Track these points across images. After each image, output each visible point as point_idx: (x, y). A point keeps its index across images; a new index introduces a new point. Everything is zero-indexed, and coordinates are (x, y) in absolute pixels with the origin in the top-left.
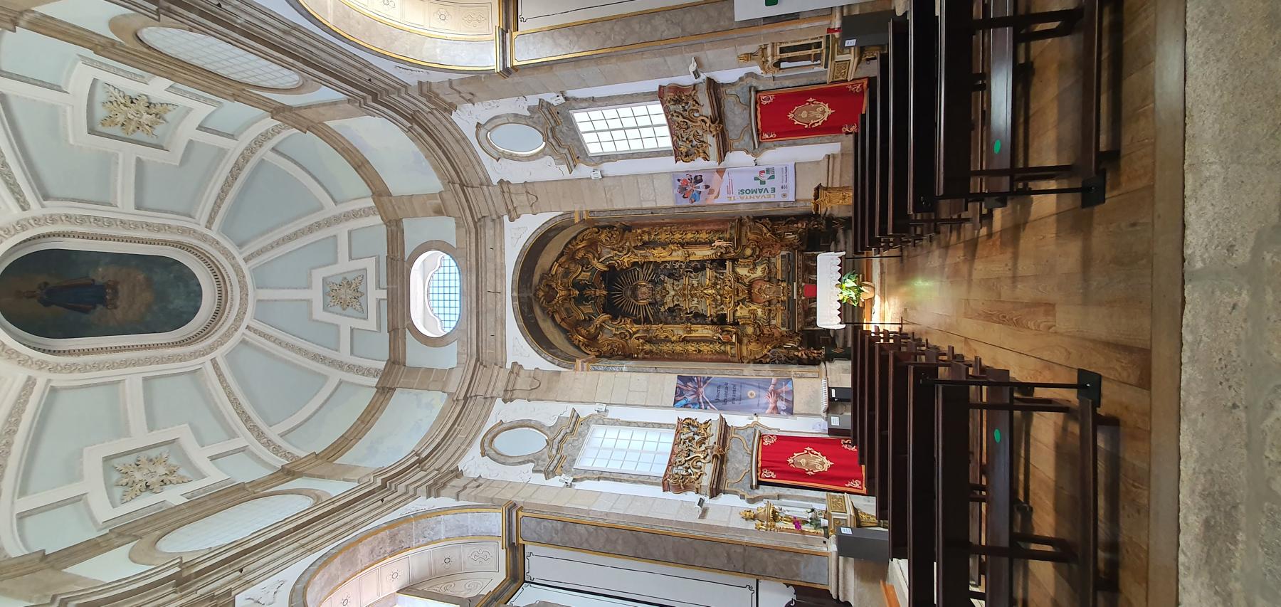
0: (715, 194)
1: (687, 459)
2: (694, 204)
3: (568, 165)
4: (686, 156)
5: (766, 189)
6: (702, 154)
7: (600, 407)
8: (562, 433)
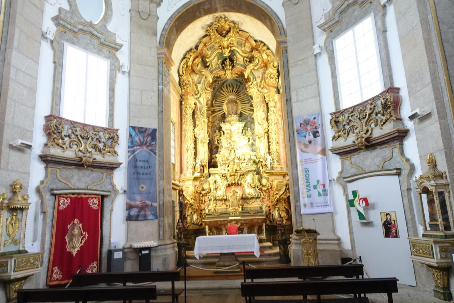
0: (304, 149)
1: (79, 137)
2: (296, 133)
3: (325, 24)
4: (336, 122)
5: (310, 190)
6: (337, 135)
7: (126, 67)
8: (99, 35)
